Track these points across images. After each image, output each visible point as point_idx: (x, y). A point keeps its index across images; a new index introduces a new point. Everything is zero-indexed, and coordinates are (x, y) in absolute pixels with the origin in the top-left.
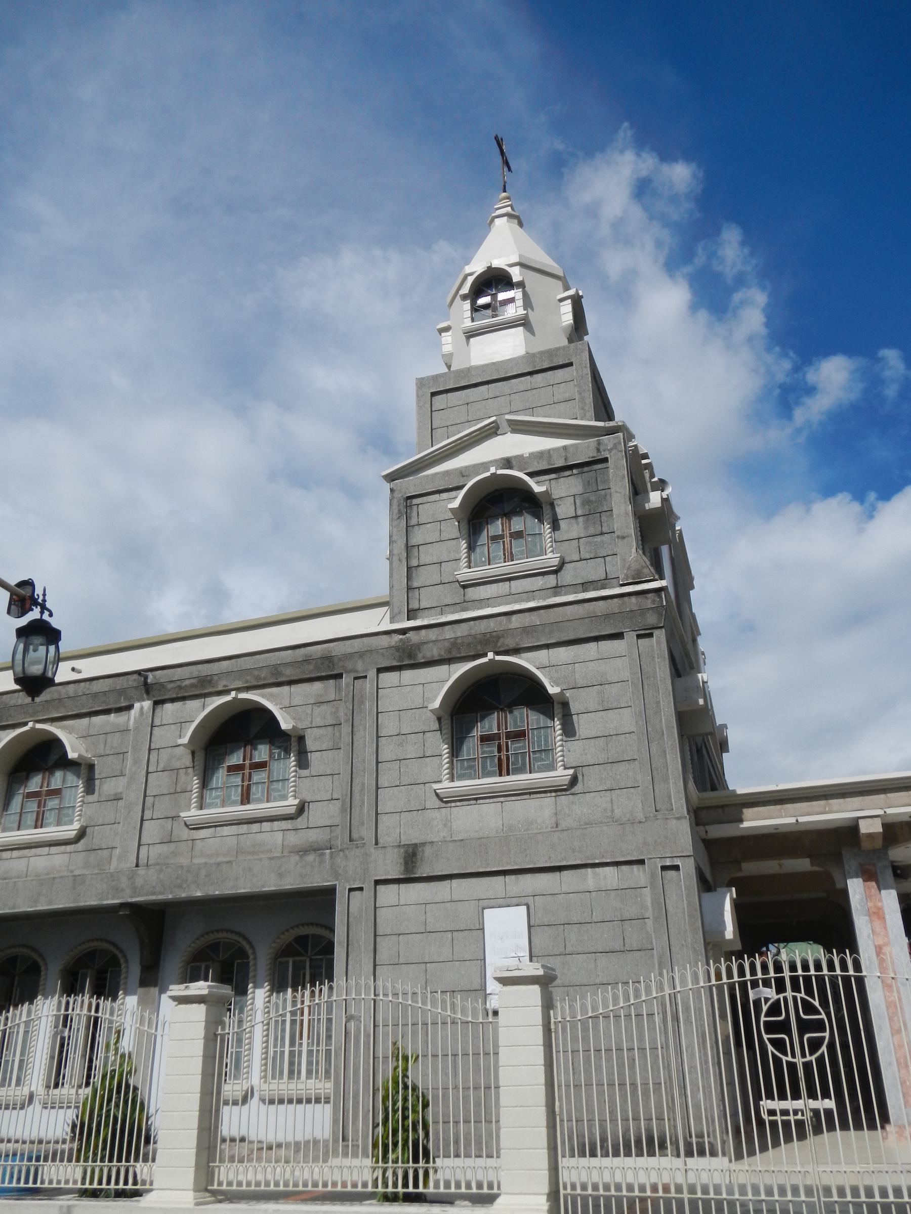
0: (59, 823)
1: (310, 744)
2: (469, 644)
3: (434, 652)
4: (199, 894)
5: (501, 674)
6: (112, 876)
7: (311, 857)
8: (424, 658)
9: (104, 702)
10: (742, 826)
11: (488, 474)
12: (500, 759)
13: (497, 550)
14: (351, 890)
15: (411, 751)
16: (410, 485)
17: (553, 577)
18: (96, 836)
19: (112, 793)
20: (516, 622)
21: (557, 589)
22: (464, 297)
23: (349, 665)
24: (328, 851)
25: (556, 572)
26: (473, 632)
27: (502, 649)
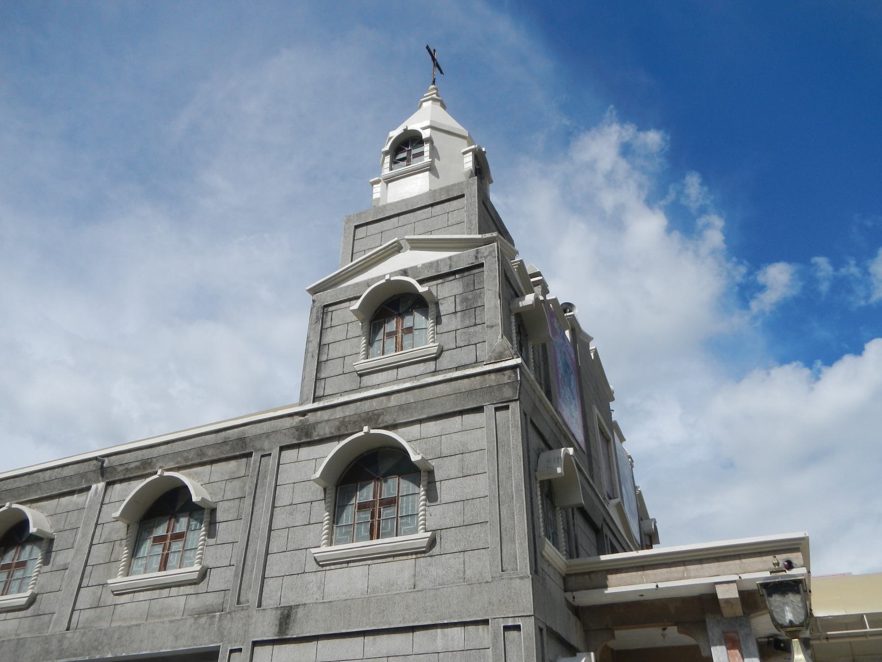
0: (19, 591)
1: (220, 516)
2: (355, 422)
3: (326, 430)
4: (109, 656)
5: (381, 448)
6: (46, 639)
7: (203, 620)
10: (606, 592)
11: (384, 281)
12: (372, 525)
13: (391, 343)
14: (232, 651)
15: (299, 519)
16: (328, 296)
17: (432, 363)
19: (62, 563)
20: (394, 400)
21: (435, 372)
22: (386, 153)
23: (258, 444)
24: (218, 614)
25: (435, 359)
26: (359, 411)
27: (381, 426)
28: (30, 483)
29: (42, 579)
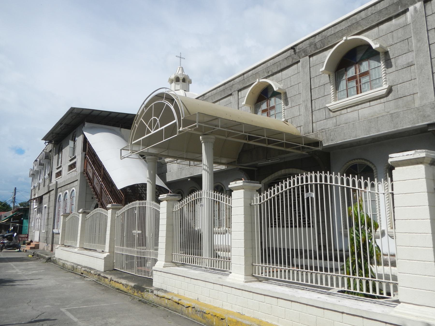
6: (418, 109)
9: (386, 14)
18: (398, 91)
19: (405, 63)
28: (349, 24)
29: (391, 77)
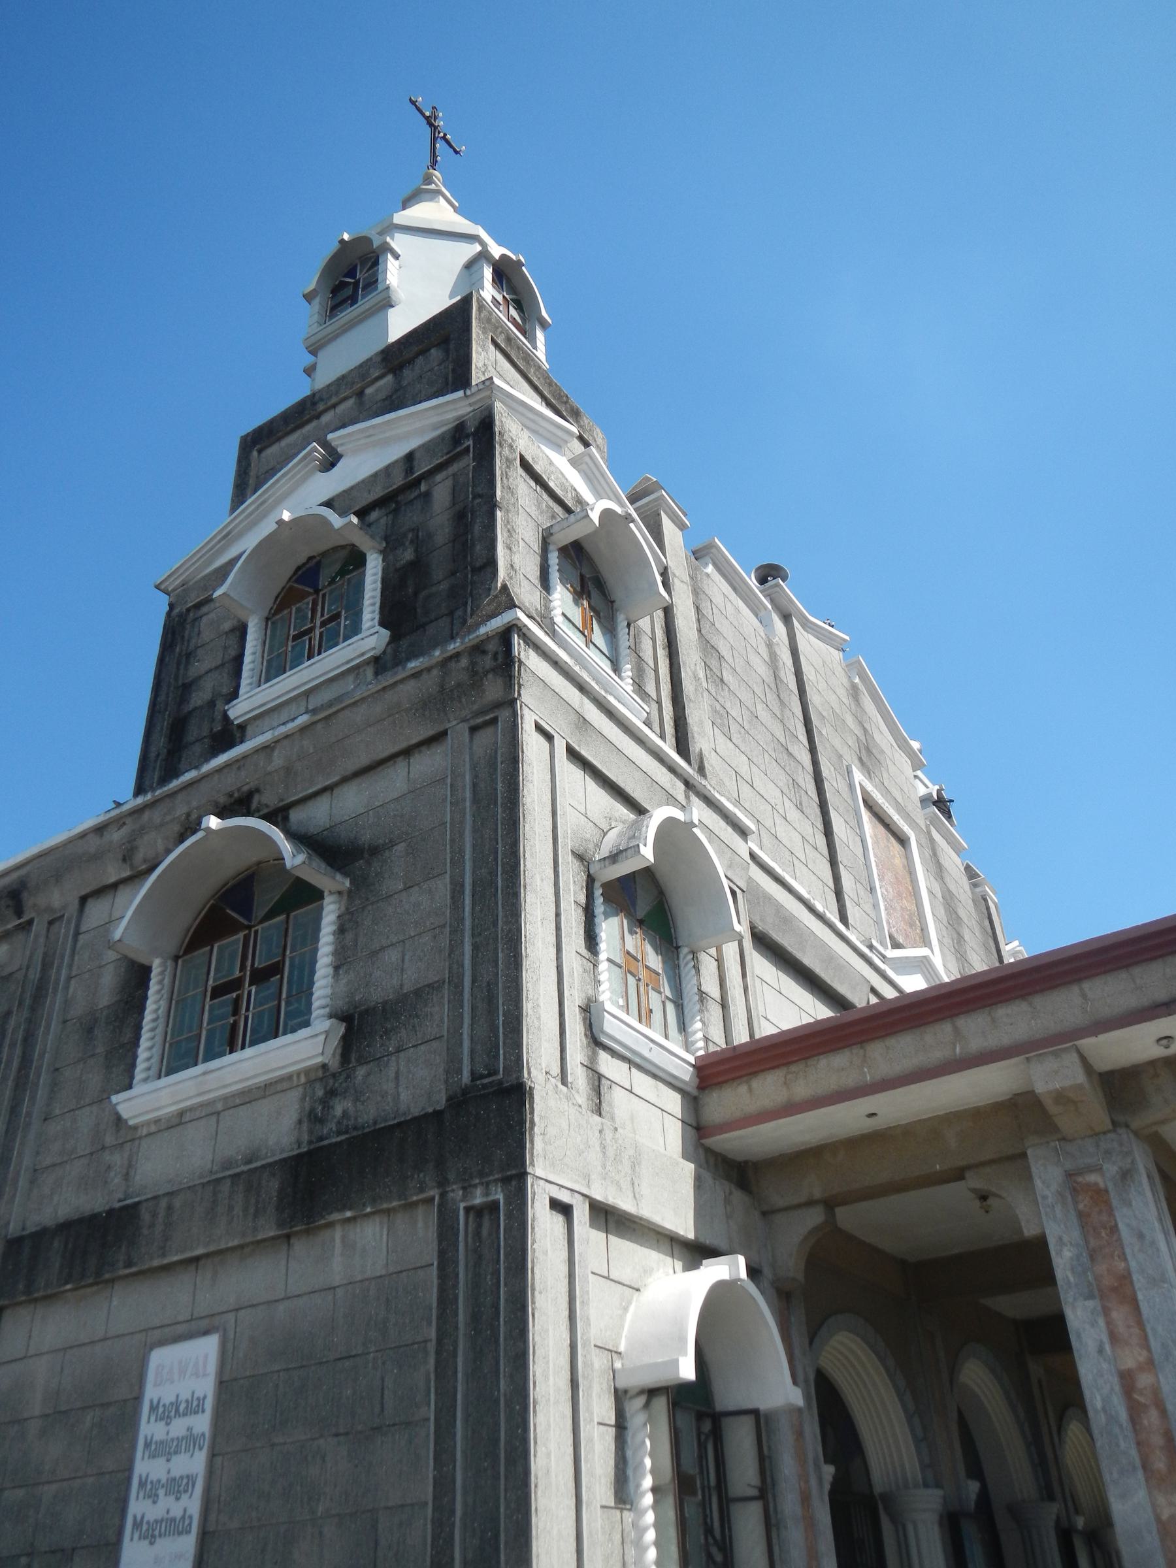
8: (145, 861)
